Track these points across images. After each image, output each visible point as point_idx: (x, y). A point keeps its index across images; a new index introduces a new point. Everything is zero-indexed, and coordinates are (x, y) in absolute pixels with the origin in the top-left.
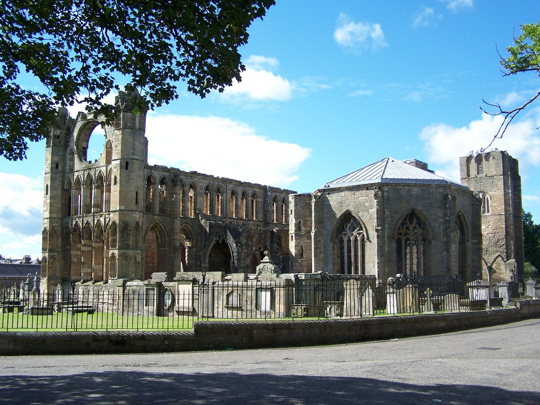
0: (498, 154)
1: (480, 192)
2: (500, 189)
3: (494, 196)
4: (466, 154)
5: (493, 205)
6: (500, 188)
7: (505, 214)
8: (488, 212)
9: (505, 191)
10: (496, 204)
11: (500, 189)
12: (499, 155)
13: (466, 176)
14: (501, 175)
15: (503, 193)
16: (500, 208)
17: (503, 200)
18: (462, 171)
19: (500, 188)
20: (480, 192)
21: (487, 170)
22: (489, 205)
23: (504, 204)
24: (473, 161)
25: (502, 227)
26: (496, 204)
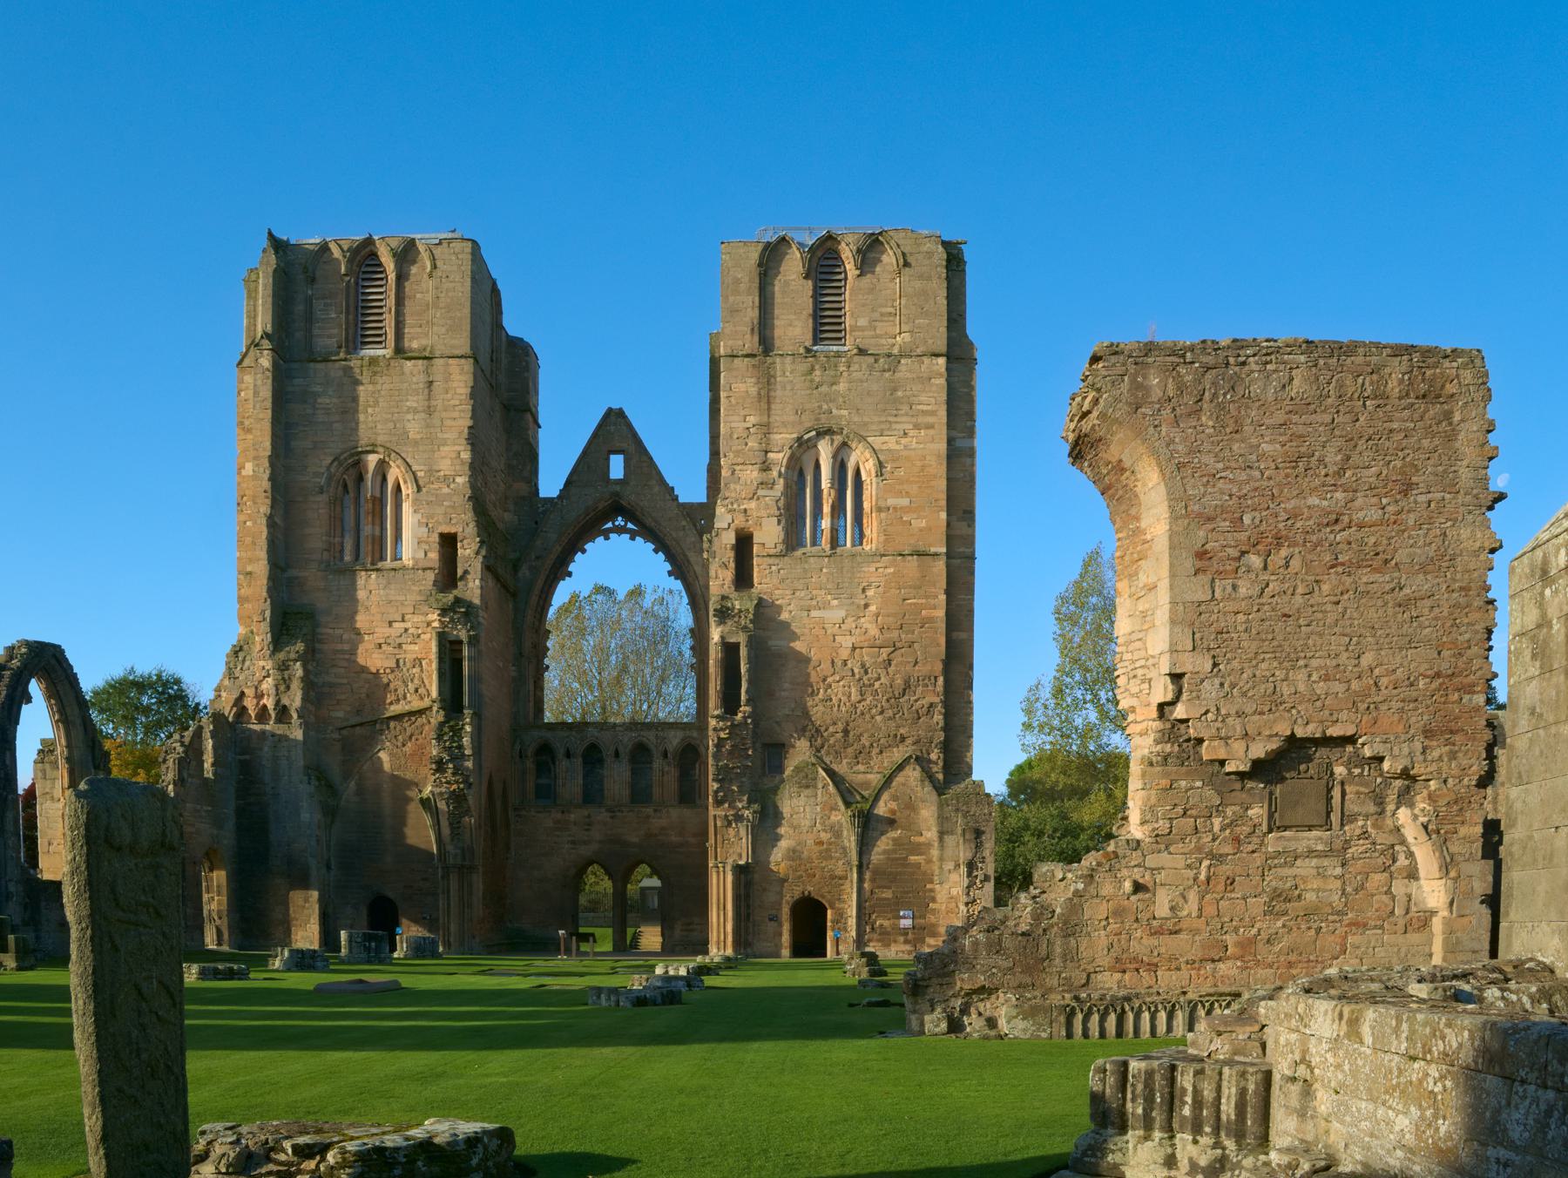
0: (928, 246)
2: (931, 426)
3: (895, 457)
5: (891, 502)
6: (930, 420)
7: (949, 555)
9: (950, 441)
10: (905, 502)
12: (930, 254)
14: (937, 355)
16: (924, 524)
17: (943, 484)
19: (930, 420)
20: (821, 434)
21: (862, 322)
22: (866, 505)
23: (944, 503)
24: (793, 266)
25: (931, 620)
26: (905, 502)
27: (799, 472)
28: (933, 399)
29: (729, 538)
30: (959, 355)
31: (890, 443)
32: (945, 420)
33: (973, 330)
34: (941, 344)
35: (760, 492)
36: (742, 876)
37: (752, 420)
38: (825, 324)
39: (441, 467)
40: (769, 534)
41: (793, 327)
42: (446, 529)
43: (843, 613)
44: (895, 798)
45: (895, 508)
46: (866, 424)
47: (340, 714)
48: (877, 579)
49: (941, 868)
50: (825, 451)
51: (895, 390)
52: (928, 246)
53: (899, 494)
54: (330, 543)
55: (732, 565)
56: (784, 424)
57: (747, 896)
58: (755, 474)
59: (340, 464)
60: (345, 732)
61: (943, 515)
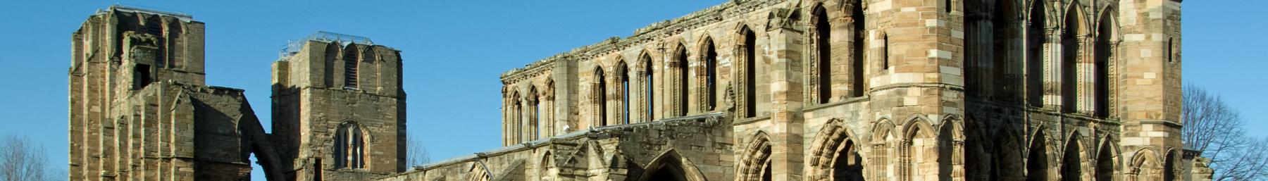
0: (390, 53)
1: (350, 123)
2: (391, 125)
3: (378, 135)
4: (329, 40)
5: (376, 153)
8: (362, 167)
9: (398, 130)
10: (382, 153)
11: (391, 125)
12: (391, 56)
13: (321, 84)
14: (394, 97)
15: (395, 133)
16: (388, 162)
18: (313, 70)
20: (350, 123)
23: (396, 155)
26: (382, 153)
27: (340, 140)
28: (392, 114)
30: (401, 97)
31: (376, 129)
32: (396, 122)
33: (405, 88)
34: (395, 93)
35: (325, 144)
37: (322, 114)
38: (350, 79)
40: (328, 162)
41: (339, 79)
45: (378, 155)
46: (366, 121)
50: (350, 130)
51: (377, 109)
52: (390, 53)
53: (379, 150)
55: (314, 172)
56: (335, 117)
58: (323, 136)
61: (396, 160)
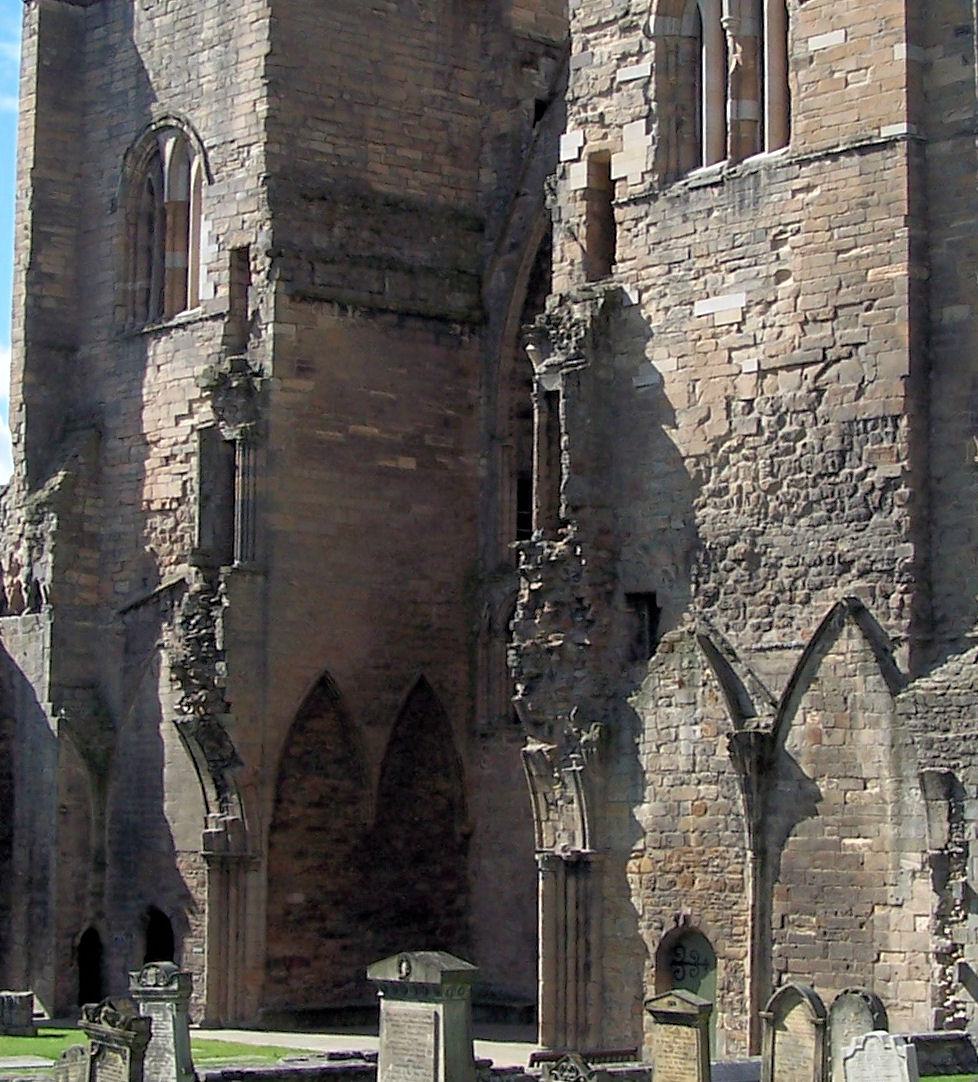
7: (918, 144)
10: (837, 37)
29: (579, 177)
36: (571, 882)
39: (236, 135)
42: (238, 241)
43: (740, 300)
44: (820, 706)
47: (123, 587)
48: (796, 216)
49: (898, 866)
54: (125, 292)
57: (583, 926)
59: (137, 159)
60: (128, 618)
61: (900, 51)
